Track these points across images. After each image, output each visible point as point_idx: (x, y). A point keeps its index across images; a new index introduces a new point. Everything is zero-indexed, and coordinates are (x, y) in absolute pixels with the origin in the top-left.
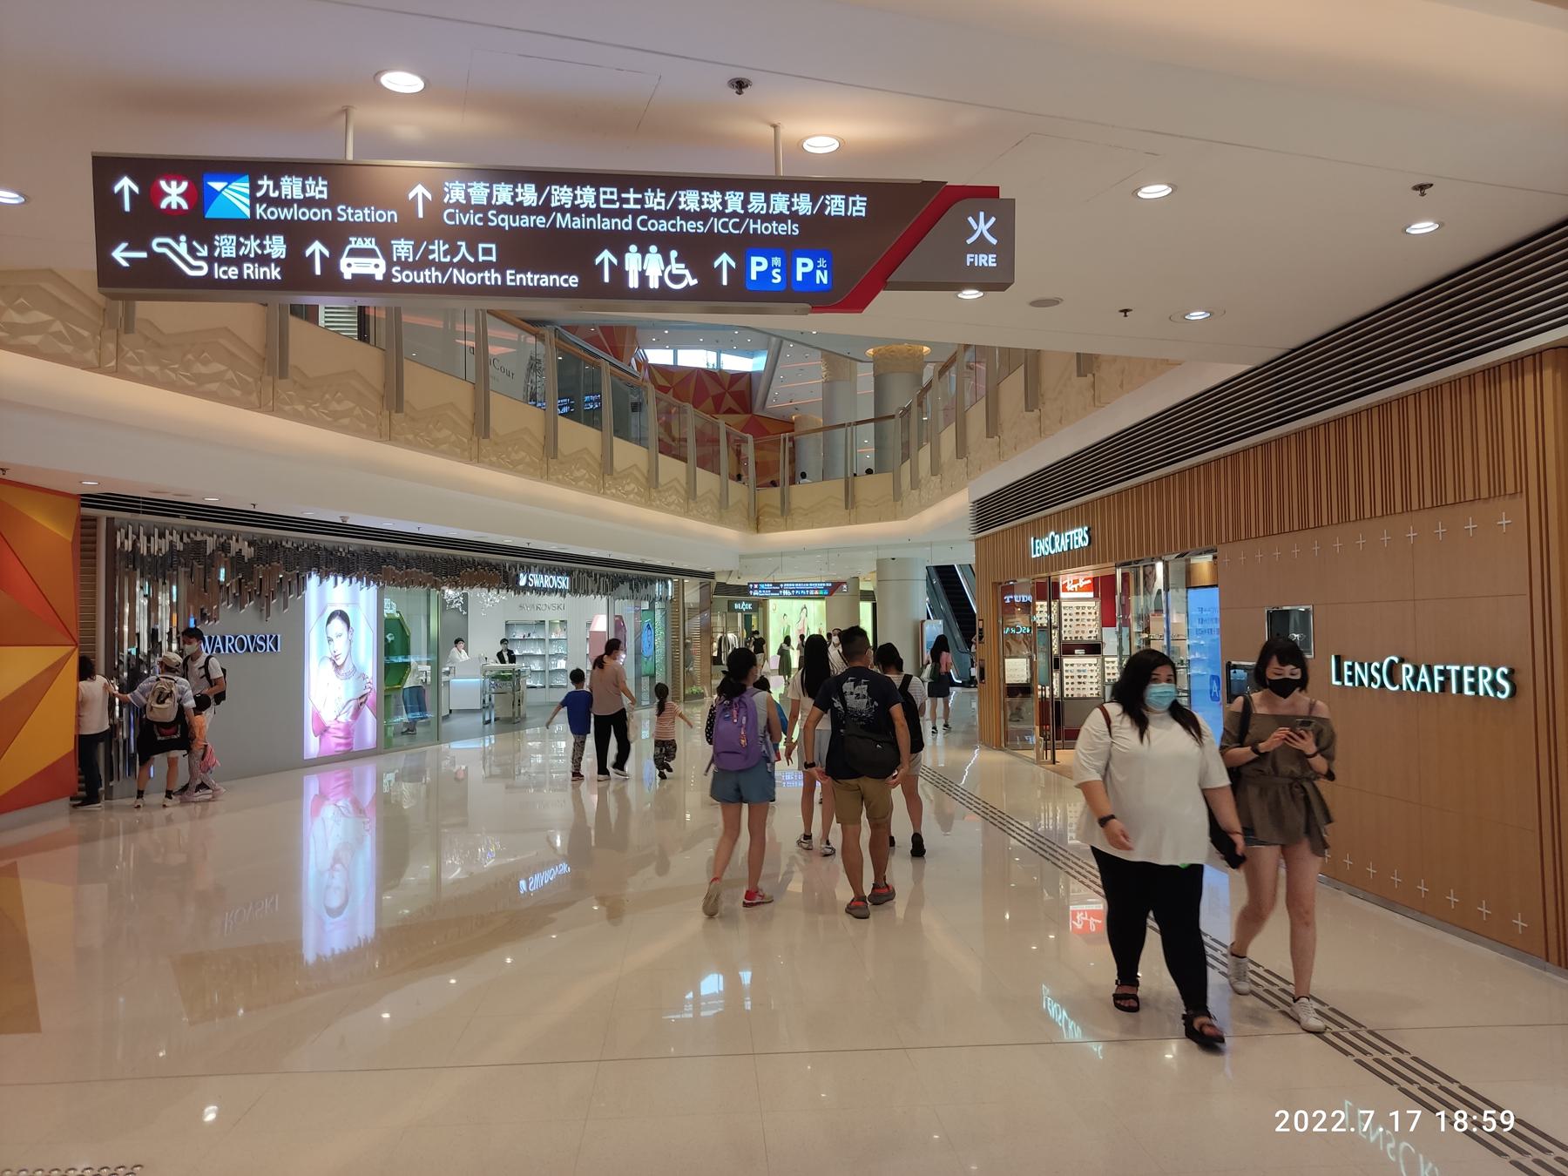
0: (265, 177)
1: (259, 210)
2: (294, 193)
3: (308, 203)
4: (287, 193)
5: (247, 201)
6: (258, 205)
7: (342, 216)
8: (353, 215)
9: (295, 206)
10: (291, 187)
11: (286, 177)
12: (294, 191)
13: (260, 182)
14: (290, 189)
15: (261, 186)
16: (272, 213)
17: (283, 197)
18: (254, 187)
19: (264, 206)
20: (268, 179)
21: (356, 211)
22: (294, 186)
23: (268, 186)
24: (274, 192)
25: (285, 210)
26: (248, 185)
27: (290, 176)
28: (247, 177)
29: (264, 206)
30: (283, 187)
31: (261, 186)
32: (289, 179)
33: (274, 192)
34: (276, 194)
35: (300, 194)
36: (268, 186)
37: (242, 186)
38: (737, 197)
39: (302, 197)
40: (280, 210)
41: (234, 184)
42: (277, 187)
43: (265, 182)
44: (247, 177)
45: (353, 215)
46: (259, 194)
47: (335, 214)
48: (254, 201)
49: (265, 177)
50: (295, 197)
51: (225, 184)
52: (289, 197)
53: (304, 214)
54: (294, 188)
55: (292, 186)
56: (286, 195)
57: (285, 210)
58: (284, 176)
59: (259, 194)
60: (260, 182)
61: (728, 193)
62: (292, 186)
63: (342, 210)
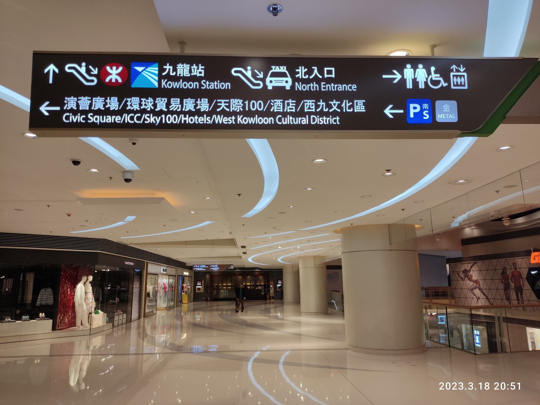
0: (168, 64)
1: (163, 83)
2: (185, 74)
3: (193, 78)
4: (180, 73)
5: (157, 78)
6: (163, 80)
7: (203, 86)
8: (209, 85)
9: (181, 80)
10: (183, 69)
11: (180, 64)
12: (185, 72)
13: (165, 67)
14: (182, 71)
15: (166, 69)
16: (170, 85)
17: (178, 75)
18: (161, 70)
19: (166, 80)
20: (170, 65)
21: (211, 83)
22: (185, 69)
23: (169, 69)
24: (173, 72)
25: (176, 83)
26: (157, 69)
27: (182, 64)
28: (157, 64)
29: (166, 80)
30: (178, 70)
31: (166, 69)
32: (182, 65)
33: (173, 72)
34: (174, 73)
35: (188, 74)
36: (169, 69)
37: (154, 69)
38: (163, 101)
39: (189, 75)
40: (173, 83)
41: (149, 68)
42: (175, 70)
43: (168, 67)
44: (157, 64)
45: (209, 85)
46: (164, 74)
47: (201, 85)
48: (160, 77)
49: (168, 64)
50: (185, 75)
51: (143, 68)
52: (182, 75)
53: (185, 85)
54: (185, 70)
55: (183, 69)
56: (180, 74)
57: (176, 83)
58: (179, 64)
59: (164, 74)
60: (165, 67)
61: (157, 99)
62: (183, 69)
63: (204, 82)
